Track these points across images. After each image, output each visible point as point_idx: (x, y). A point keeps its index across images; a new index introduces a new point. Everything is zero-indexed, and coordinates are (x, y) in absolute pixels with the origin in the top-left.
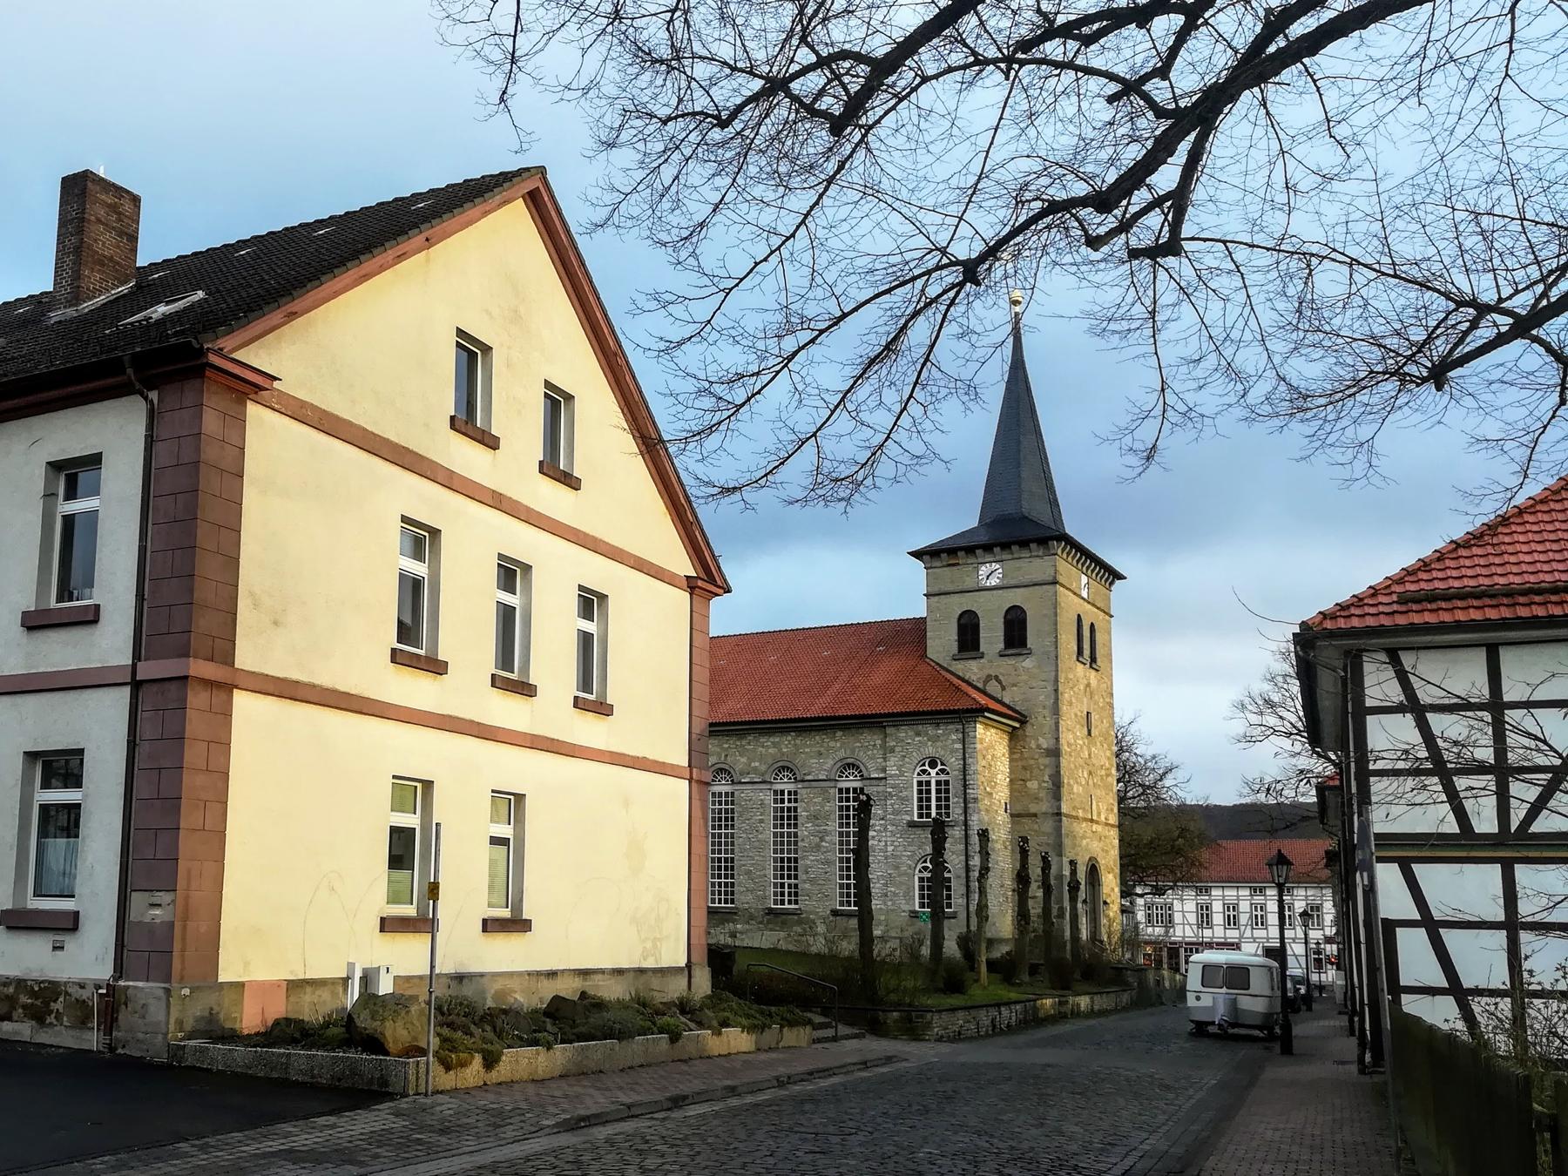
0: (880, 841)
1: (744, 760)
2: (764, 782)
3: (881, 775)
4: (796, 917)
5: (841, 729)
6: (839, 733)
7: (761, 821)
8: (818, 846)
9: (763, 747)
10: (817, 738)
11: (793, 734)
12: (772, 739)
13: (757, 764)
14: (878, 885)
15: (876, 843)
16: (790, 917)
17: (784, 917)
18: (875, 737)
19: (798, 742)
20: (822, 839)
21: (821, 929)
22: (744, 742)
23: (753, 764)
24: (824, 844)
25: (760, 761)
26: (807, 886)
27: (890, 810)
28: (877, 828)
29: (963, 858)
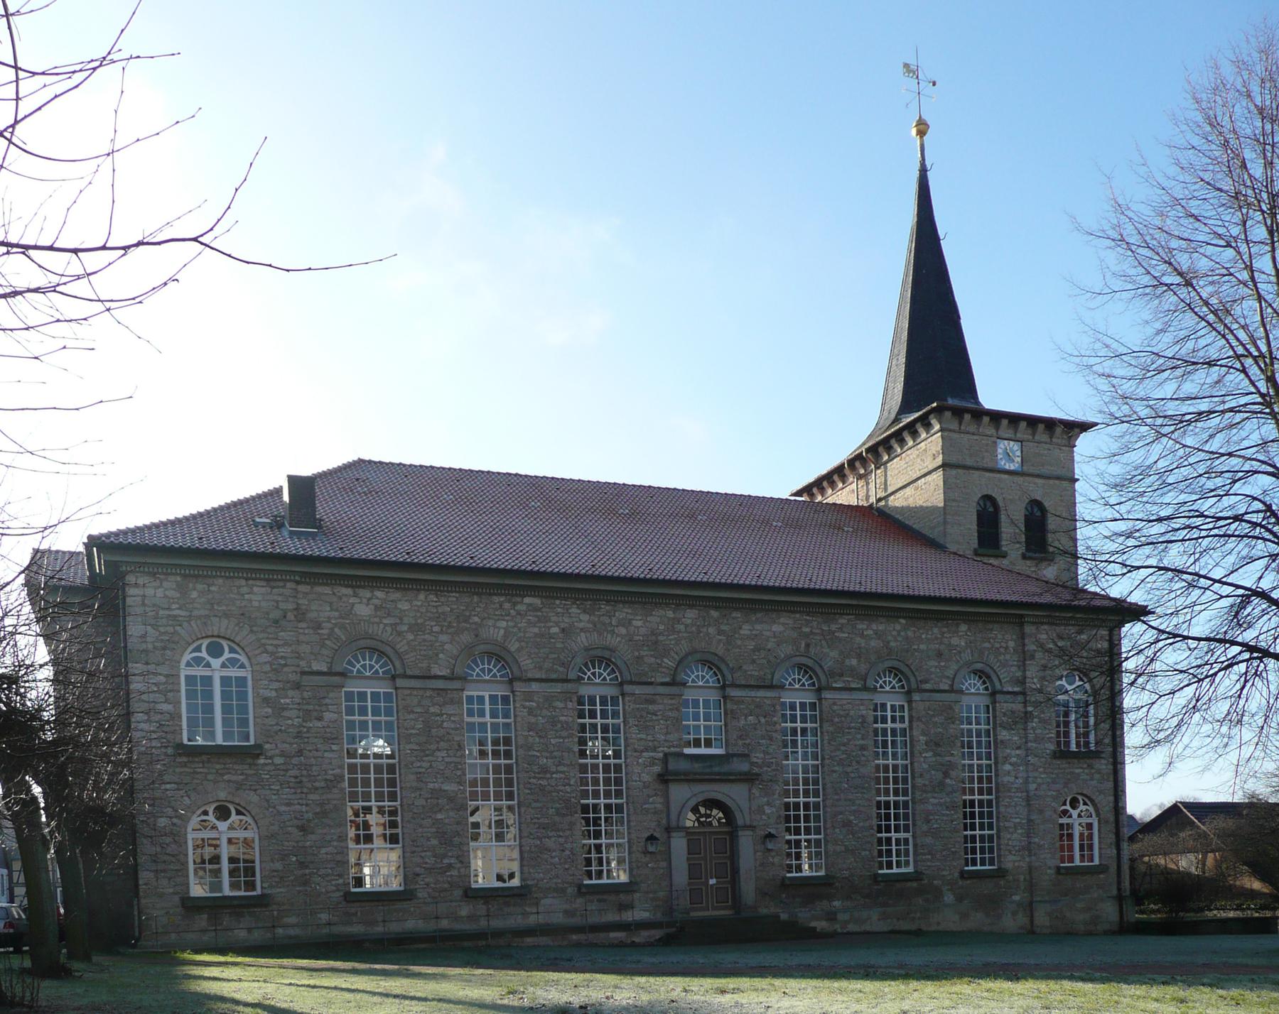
0: (1017, 778)
1: (834, 654)
2: (865, 688)
3: (1016, 689)
4: (915, 884)
5: (965, 621)
6: (963, 627)
7: (863, 748)
8: (942, 784)
9: (862, 636)
10: (936, 630)
11: (903, 621)
12: (874, 627)
13: (854, 662)
14: (1015, 836)
15: (1012, 779)
16: (909, 884)
17: (898, 885)
18: (1008, 636)
19: (910, 634)
20: (946, 775)
21: (949, 898)
22: (834, 627)
23: (847, 662)
24: (948, 781)
25: (859, 656)
26: (929, 840)
27: (1031, 736)
28: (1014, 759)
29: (1112, 798)
